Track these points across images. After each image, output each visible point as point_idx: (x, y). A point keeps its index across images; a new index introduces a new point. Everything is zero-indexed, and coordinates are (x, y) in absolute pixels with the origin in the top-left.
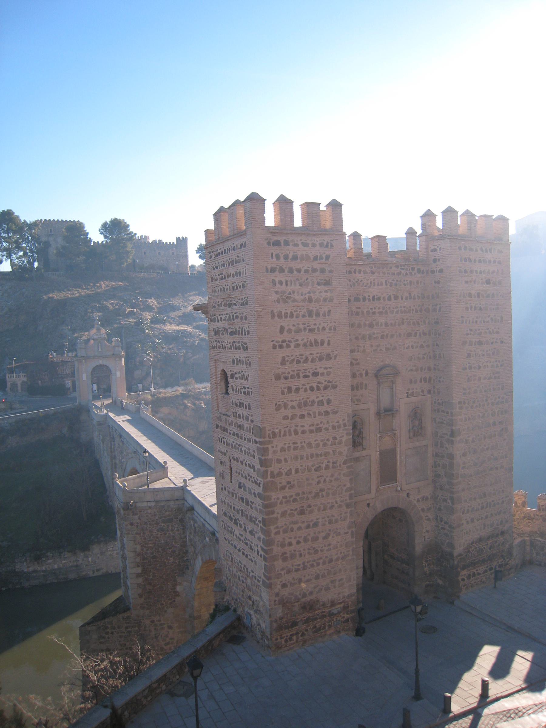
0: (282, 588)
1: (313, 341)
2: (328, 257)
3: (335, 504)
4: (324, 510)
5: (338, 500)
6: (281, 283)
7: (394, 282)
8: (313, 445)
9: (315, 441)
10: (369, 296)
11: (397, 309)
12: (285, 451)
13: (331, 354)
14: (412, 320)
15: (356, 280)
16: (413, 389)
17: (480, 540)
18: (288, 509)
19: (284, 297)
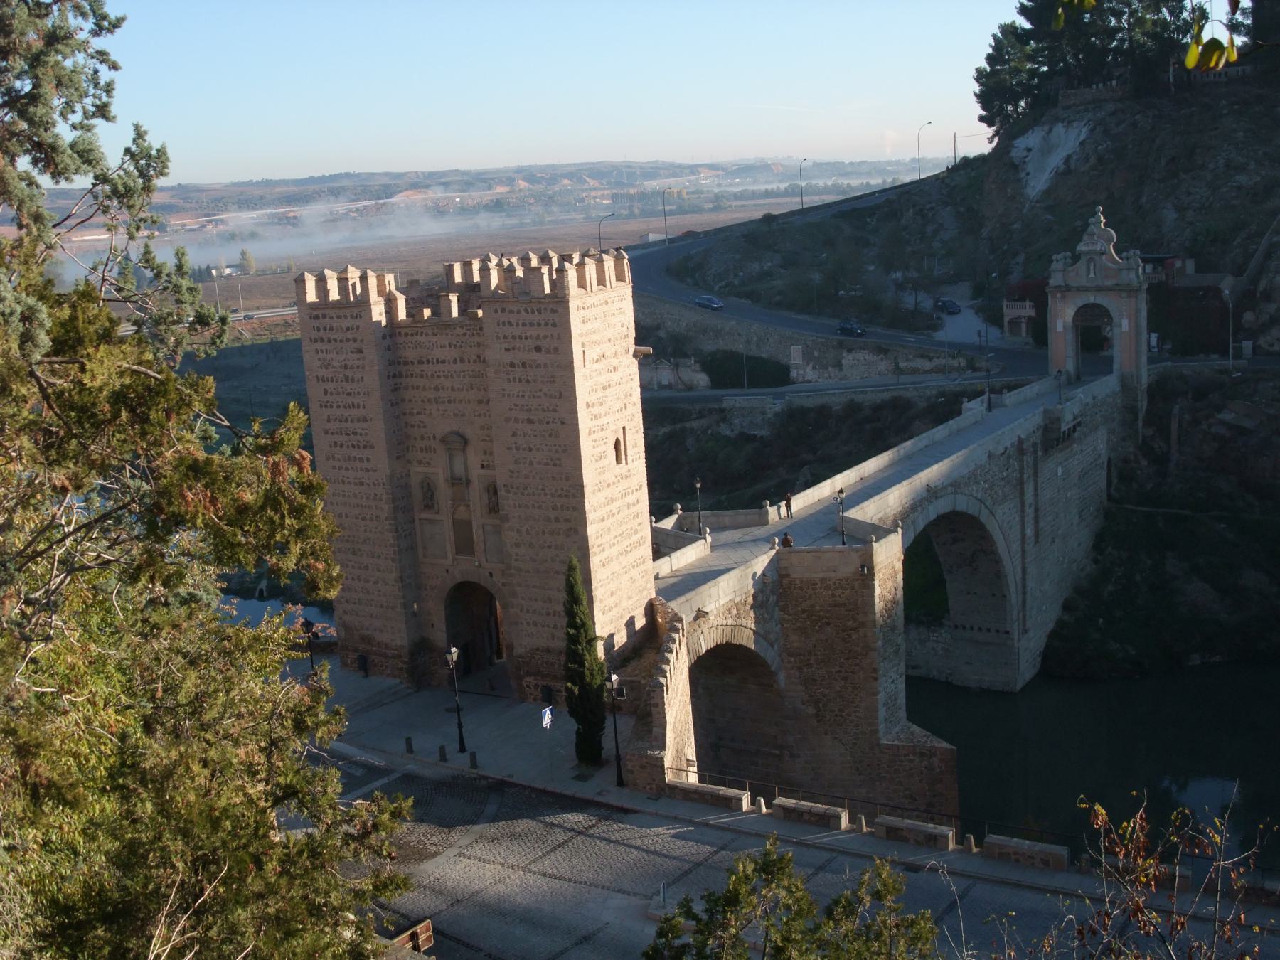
2: (358, 327)
17: (548, 650)
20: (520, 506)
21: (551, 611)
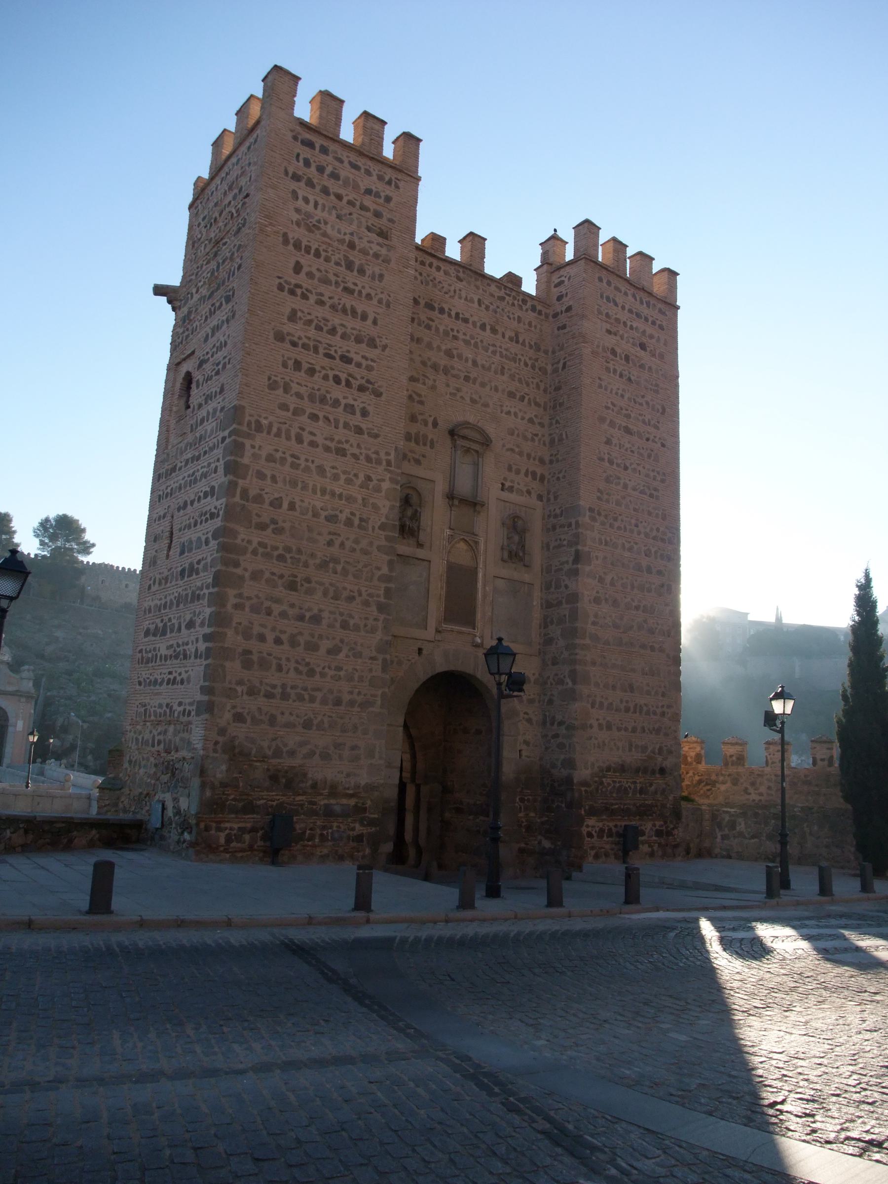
0: (234, 722)
1: (348, 307)
3: (356, 594)
4: (336, 597)
5: (363, 589)
6: (306, 200)
7: (492, 307)
8: (329, 475)
9: (333, 468)
10: (450, 310)
11: (495, 348)
12: (275, 462)
13: (378, 340)
14: (518, 374)
15: (431, 278)
16: (512, 481)
17: (622, 769)
18: (266, 569)
19: (308, 222)
20: (606, 544)
21: (631, 705)
